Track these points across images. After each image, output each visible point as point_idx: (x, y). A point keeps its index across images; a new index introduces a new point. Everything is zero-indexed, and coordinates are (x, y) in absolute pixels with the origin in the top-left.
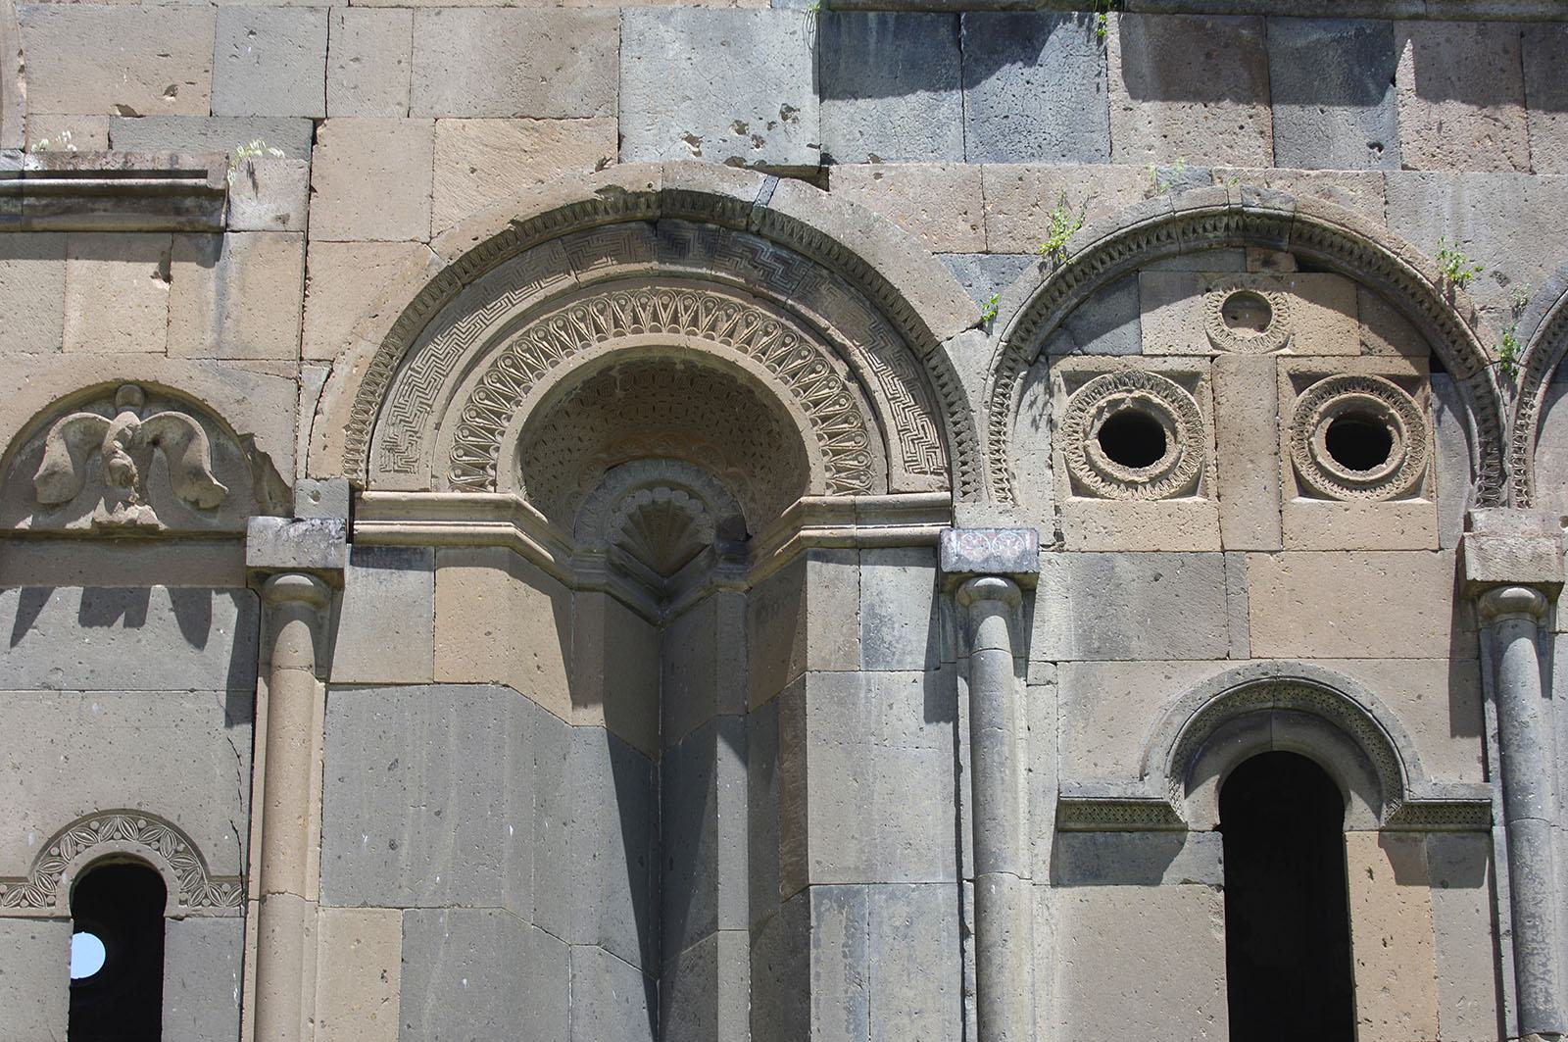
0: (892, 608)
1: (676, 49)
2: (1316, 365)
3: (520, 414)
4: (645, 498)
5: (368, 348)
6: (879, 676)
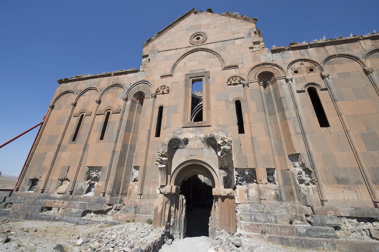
1: (263, 56)
2: (307, 67)
3: (258, 74)
5: (248, 73)
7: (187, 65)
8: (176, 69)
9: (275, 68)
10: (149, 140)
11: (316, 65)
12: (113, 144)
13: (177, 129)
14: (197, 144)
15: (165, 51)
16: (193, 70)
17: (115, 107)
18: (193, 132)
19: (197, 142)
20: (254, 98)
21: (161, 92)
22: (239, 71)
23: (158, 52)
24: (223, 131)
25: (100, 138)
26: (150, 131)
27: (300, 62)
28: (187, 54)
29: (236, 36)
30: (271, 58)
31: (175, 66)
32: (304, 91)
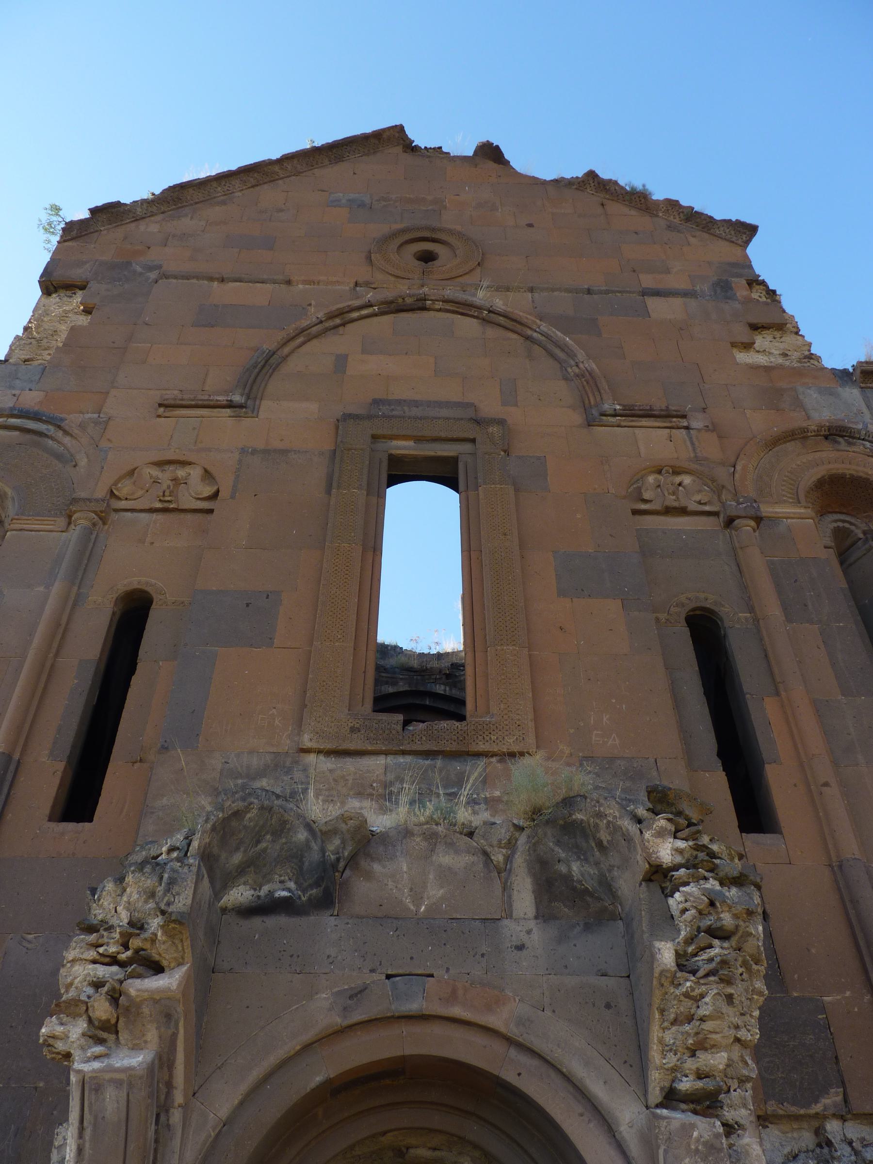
4: (835, 525)
14: (445, 875)
16: (399, 402)
19: (445, 858)
20: (806, 605)
22: (693, 444)
28: (355, 315)
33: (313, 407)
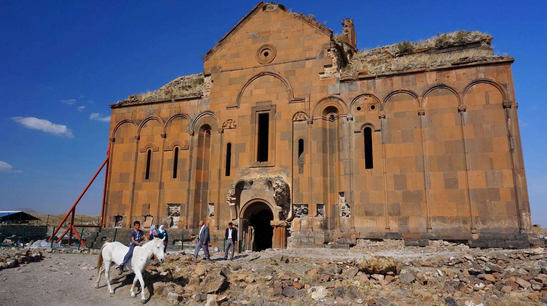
0: (344, 121)
6: (344, 125)
7: (254, 93)
8: (242, 99)
9: (341, 102)
10: (220, 178)
11: (378, 102)
12: (187, 182)
13: (245, 169)
15: (230, 71)
17: (183, 143)
18: (259, 172)
19: (260, 183)
21: (228, 127)
23: (222, 72)
24: (284, 172)
25: (173, 176)
26: (220, 171)
27: (365, 97)
28: (253, 79)
29: (308, 55)
30: (339, 90)
31: (240, 95)
32: (360, 132)
33: (248, 104)
